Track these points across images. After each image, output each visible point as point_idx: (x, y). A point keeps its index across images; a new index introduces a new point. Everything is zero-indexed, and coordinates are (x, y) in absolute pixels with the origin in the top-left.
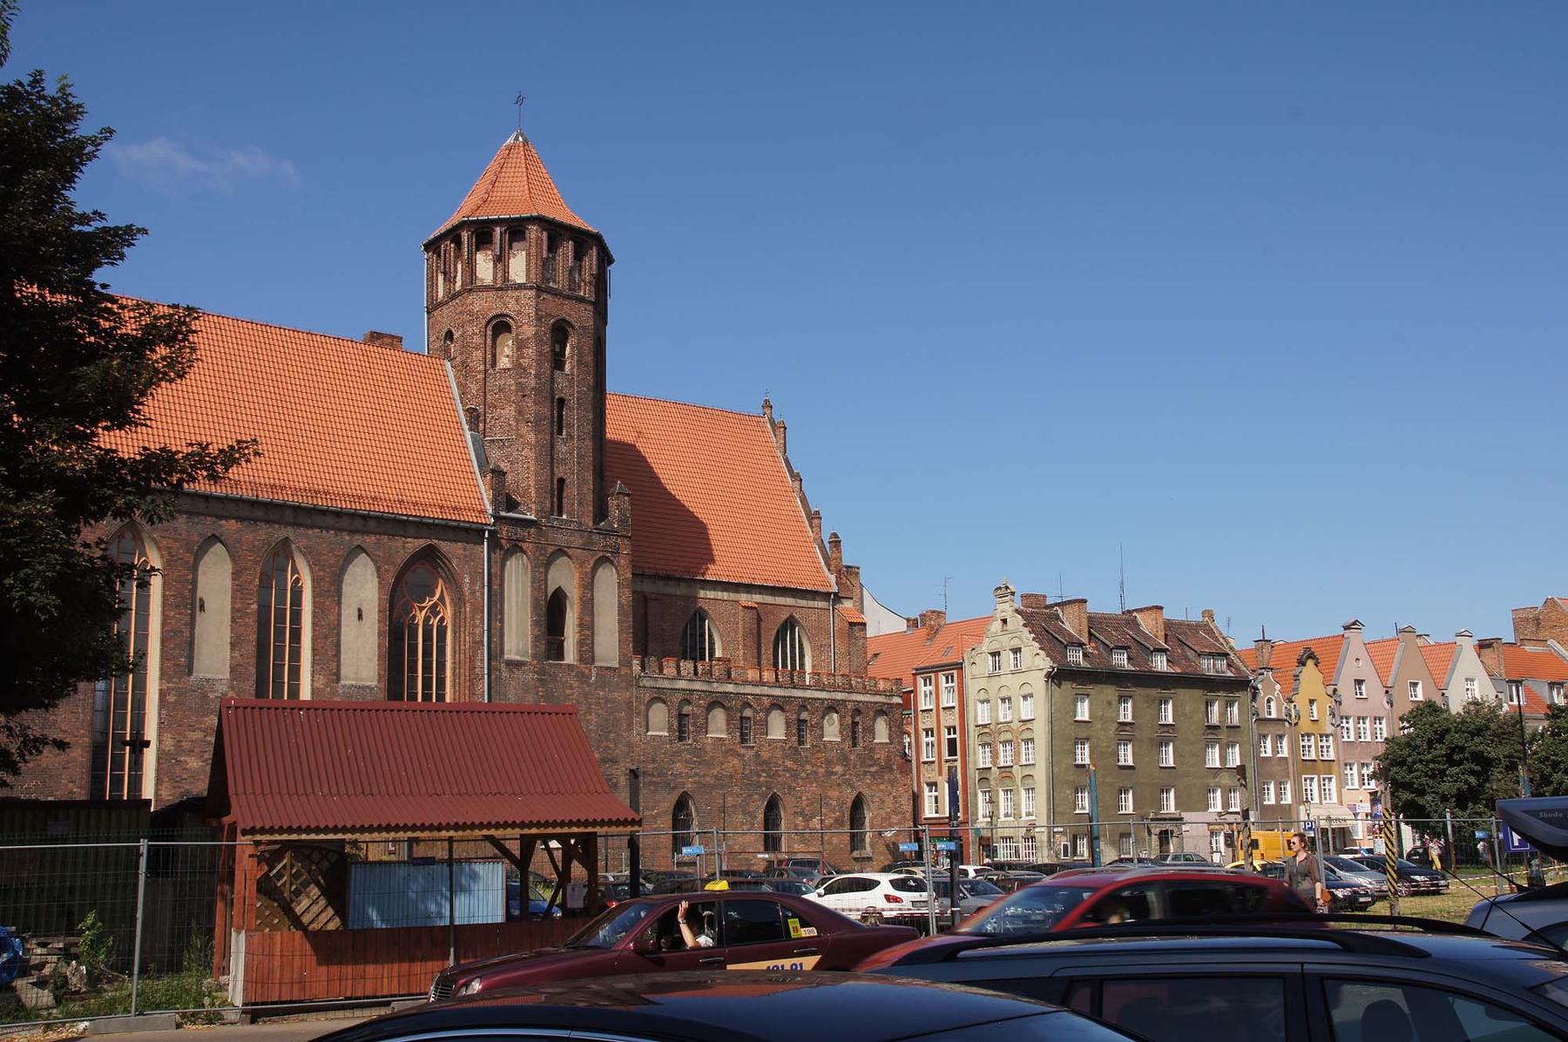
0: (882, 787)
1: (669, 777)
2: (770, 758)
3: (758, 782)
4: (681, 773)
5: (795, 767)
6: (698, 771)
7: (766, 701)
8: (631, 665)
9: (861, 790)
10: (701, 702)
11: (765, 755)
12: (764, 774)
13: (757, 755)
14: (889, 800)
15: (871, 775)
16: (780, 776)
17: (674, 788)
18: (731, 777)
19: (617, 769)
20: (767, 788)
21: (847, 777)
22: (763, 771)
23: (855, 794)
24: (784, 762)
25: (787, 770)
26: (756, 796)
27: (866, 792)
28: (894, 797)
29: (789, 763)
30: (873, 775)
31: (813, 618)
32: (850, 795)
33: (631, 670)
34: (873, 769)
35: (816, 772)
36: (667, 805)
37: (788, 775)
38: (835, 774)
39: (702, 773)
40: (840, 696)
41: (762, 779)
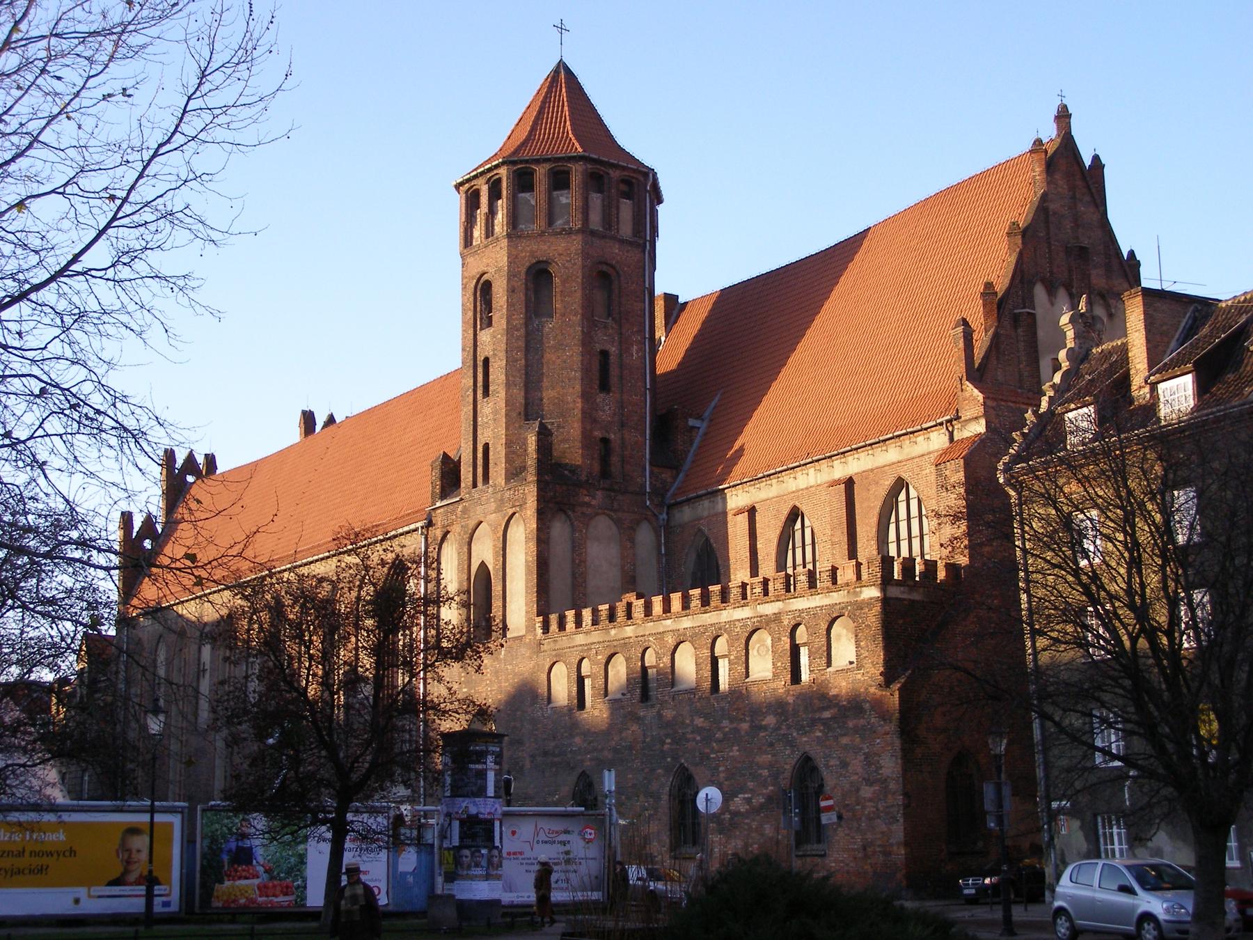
0: (845, 741)
1: (569, 756)
2: (675, 717)
3: (662, 751)
4: (580, 748)
5: (706, 725)
6: (595, 744)
7: (670, 640)
8: (535, 630)
9: (807, 748)
10: (599, 657)
11: (669, 714)
12: (668, 741)
13: (660, 715)
14: (857, 764)
15: (824, 724)
16: (688, 740)
17: (573, 768)
18: (631, 748)
19: (523, 750)
20: (673, 758)
21: (782, 732)
22: (667, 736)
23: (797, 755)
24: (692, 721)
25: (699, 730)
26: (660, 771)
27: (816, 752)
28: (867, 756)
29: (699, 721)
30: (825, 722)
31: (928, 471)
32: (788, 761)
33: (535, 635)
34: (827, 714)
35: (737, 730)
36: (567, 788)
37: (698, 738)
38: (765, 728)
39: (600, 747)
40: (769, 609)
41: (666, 747)
